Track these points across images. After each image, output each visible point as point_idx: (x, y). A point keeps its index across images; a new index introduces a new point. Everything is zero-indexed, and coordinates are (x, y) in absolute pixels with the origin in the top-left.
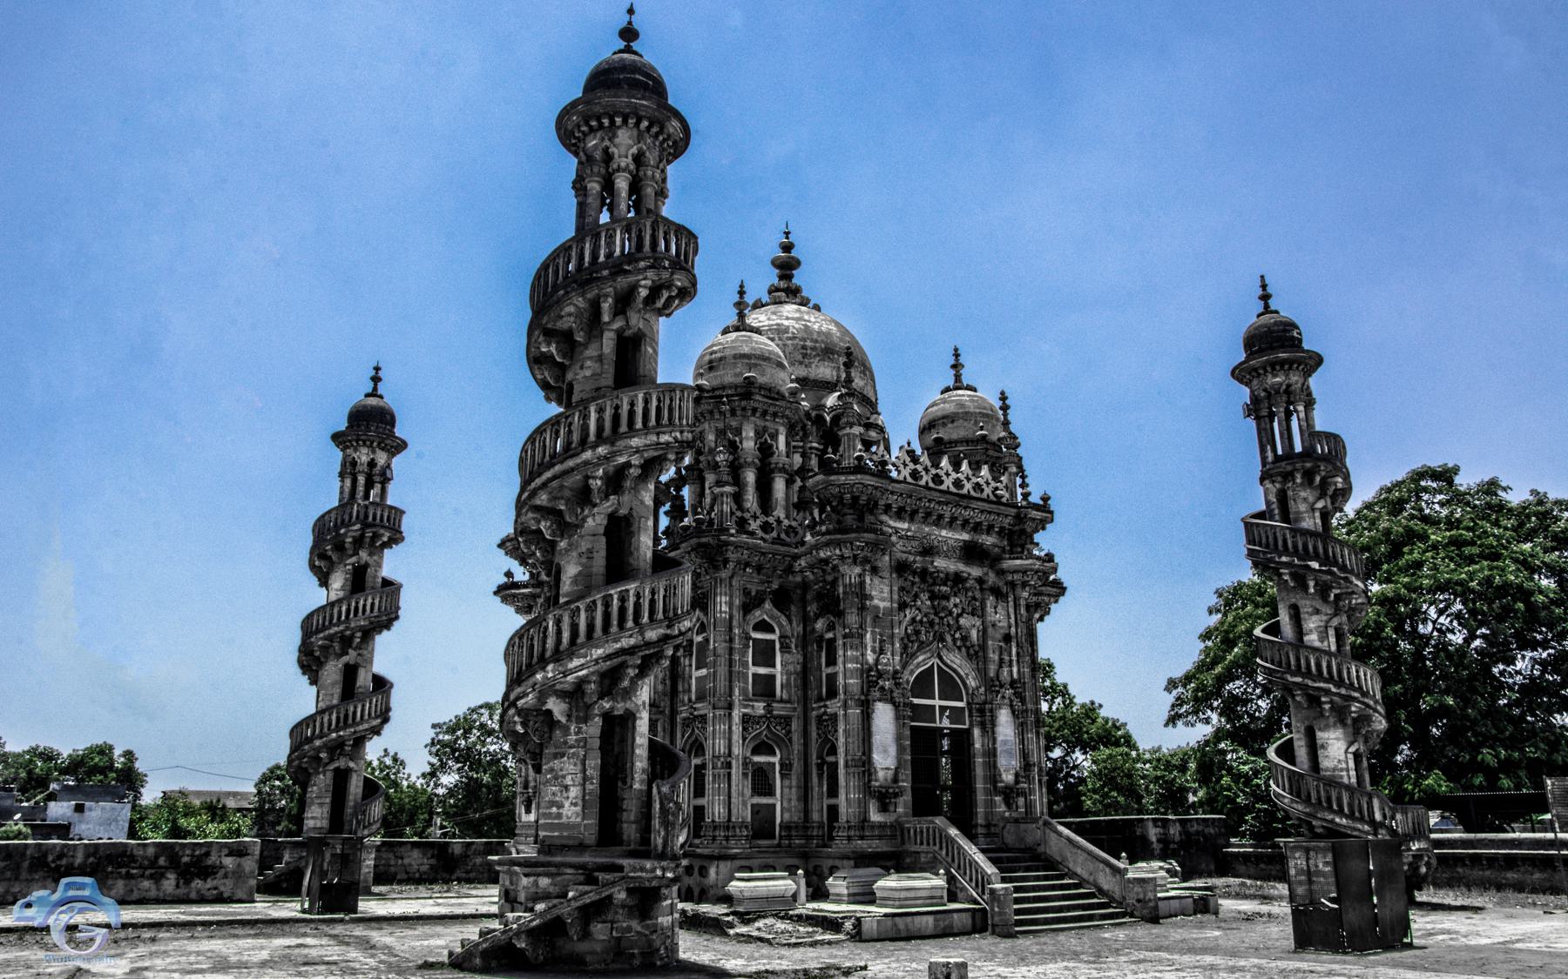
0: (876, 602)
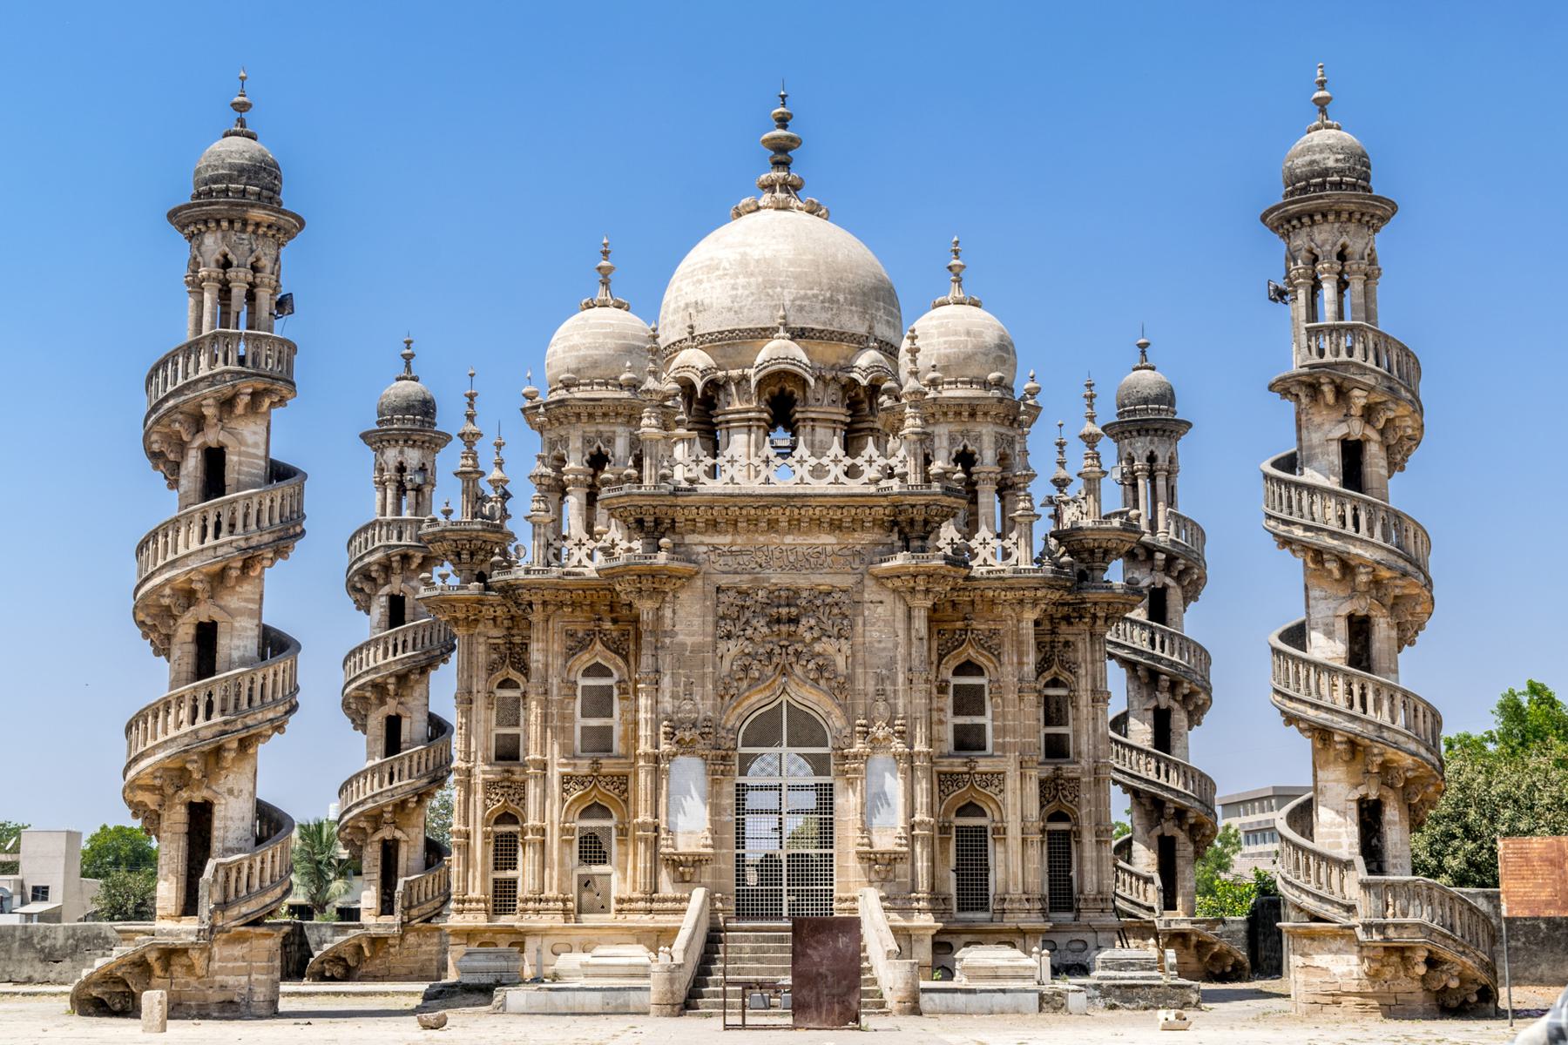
0: (680, 638)
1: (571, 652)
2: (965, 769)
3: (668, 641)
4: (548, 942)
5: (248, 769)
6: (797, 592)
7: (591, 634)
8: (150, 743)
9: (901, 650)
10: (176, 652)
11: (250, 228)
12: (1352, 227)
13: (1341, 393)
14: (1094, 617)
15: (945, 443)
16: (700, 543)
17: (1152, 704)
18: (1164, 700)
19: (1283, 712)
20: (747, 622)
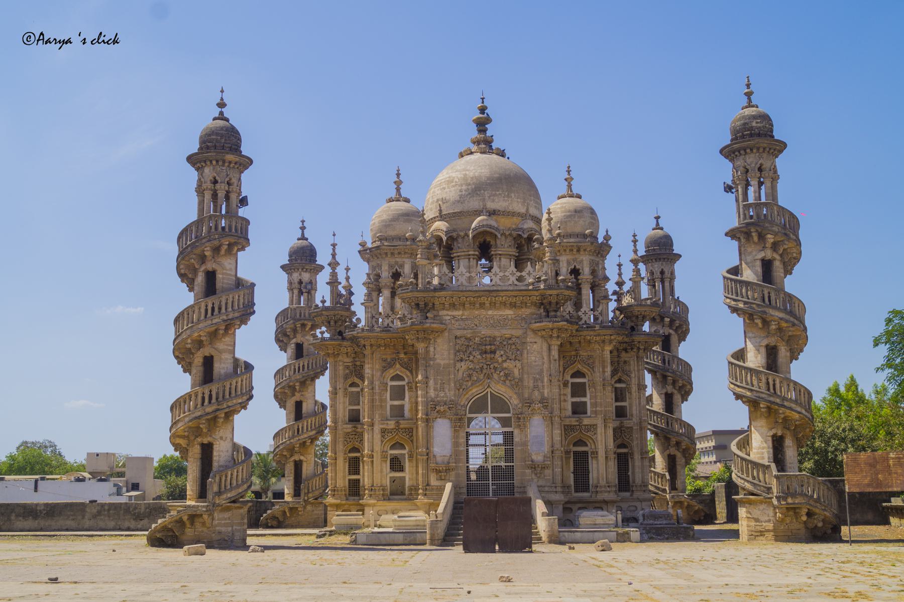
0: (438, 361)
1: (384, 369)
3: (432, 363)
4: (378, 508)
5: (230, 427)
6: (494, 338)
7: (394, 360)
8: (182, 415)
9: (546, 366)
10: (194, 371)
11: (227, 164)
12: (765, 155)
13: (762, 237)
14: (639, 349)
15: (565, 265)
16: (447, 315)
17: (664, 391)
18: (670, 389)
19: (734, 394)
20: (470, 353)
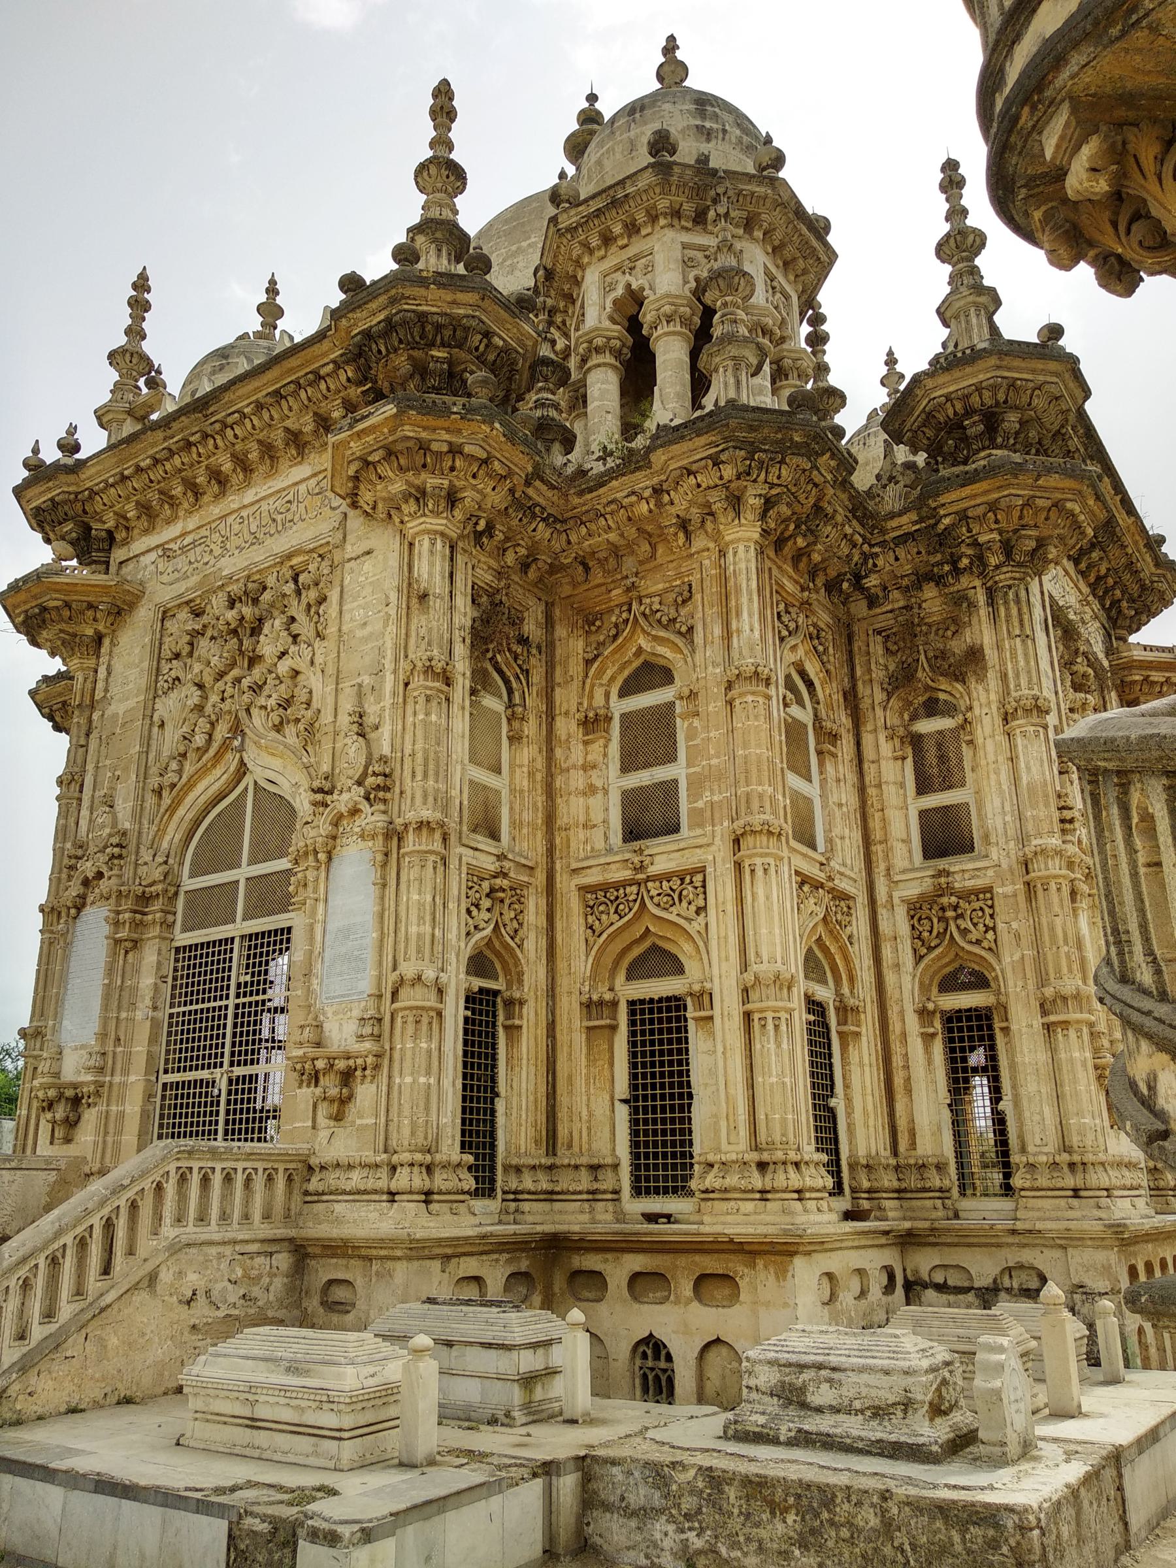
2: (627, 874)
